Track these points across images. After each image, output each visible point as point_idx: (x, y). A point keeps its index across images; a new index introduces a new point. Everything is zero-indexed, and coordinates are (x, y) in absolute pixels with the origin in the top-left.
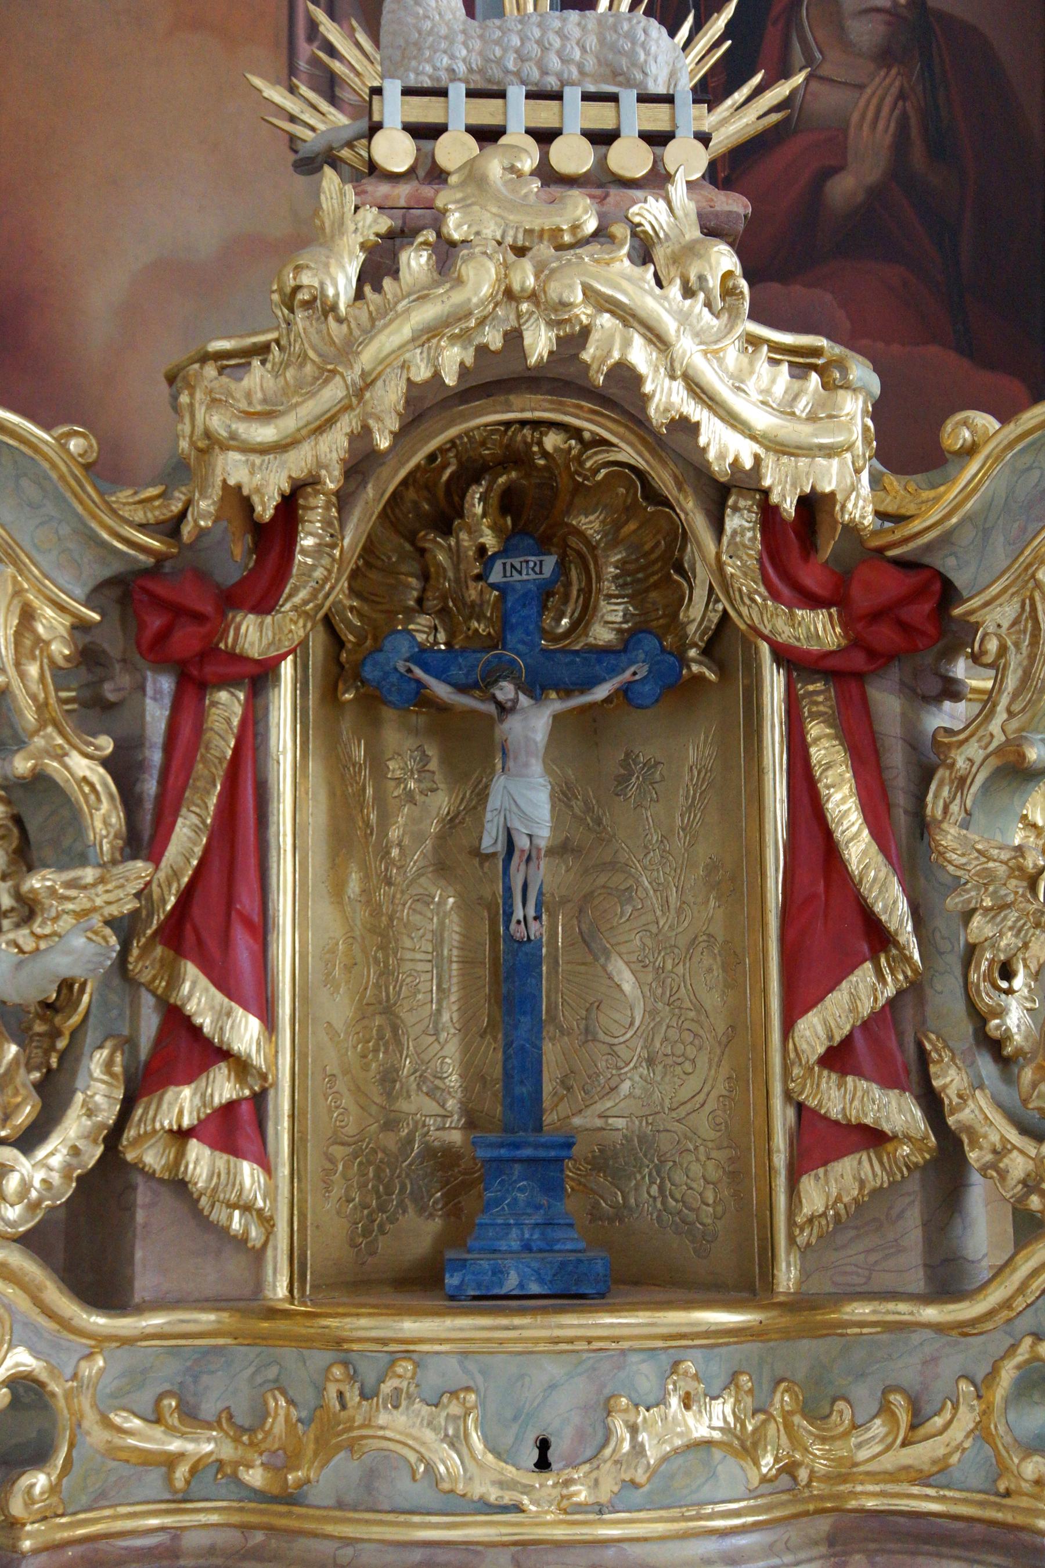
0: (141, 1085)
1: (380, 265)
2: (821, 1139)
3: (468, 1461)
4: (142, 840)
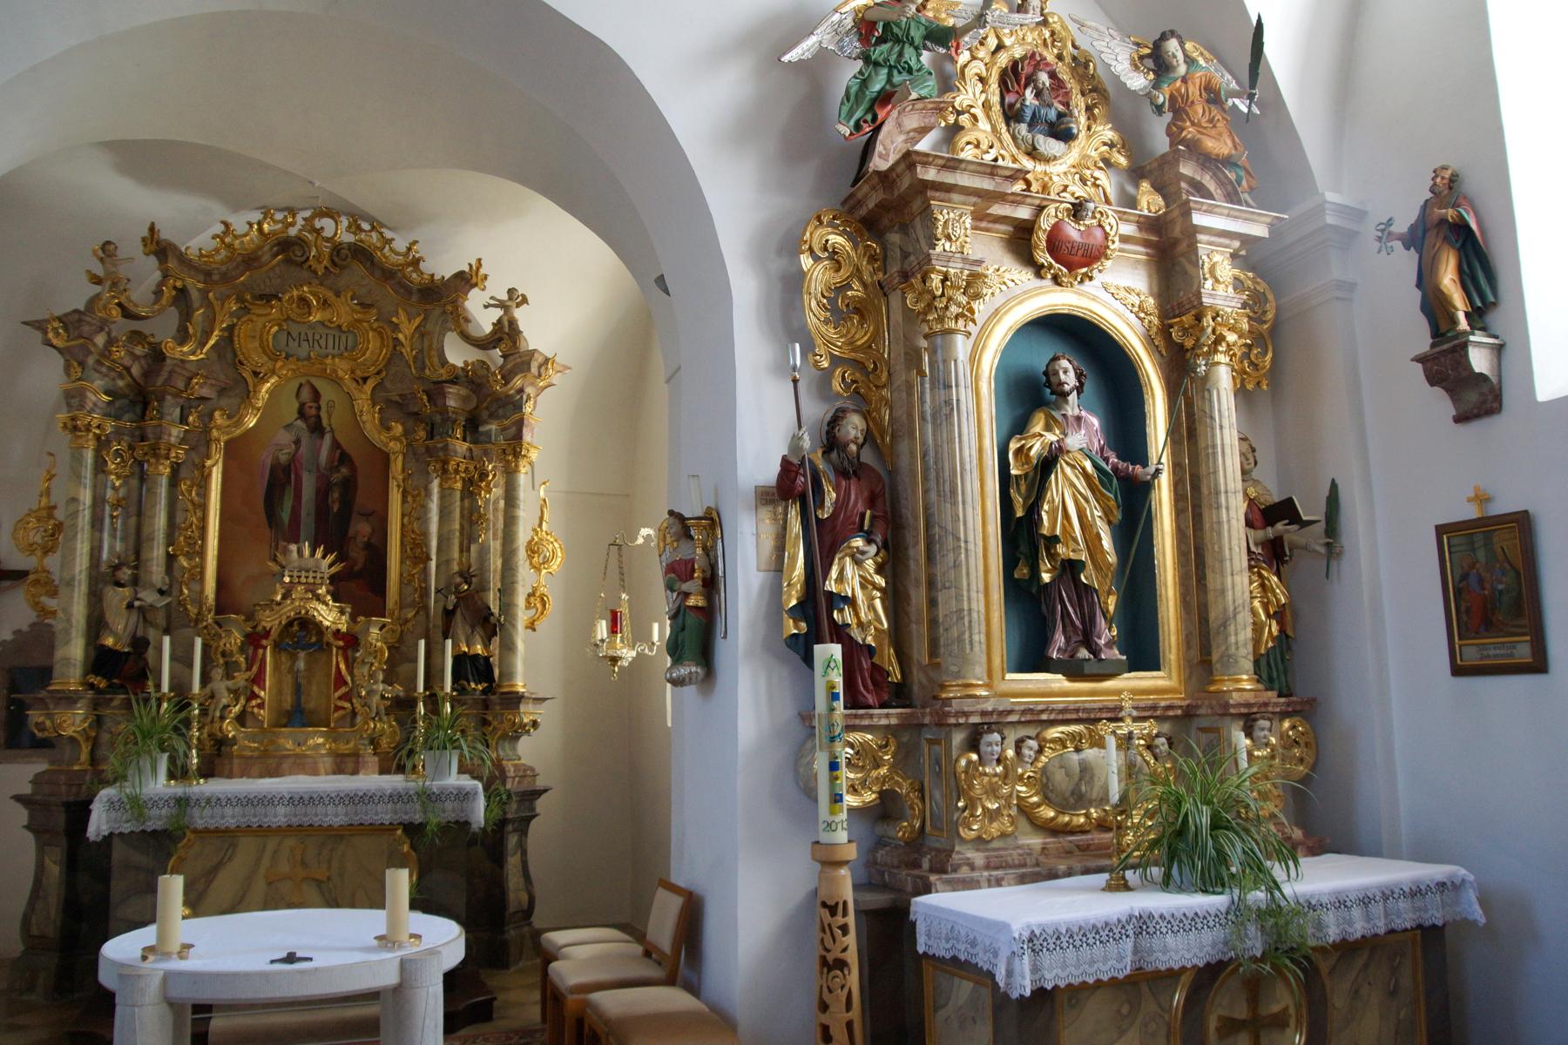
0: (248, 700)
1: (284, 597)
2: (338, 708)
3: (289, 745)
4: (249, 668)
